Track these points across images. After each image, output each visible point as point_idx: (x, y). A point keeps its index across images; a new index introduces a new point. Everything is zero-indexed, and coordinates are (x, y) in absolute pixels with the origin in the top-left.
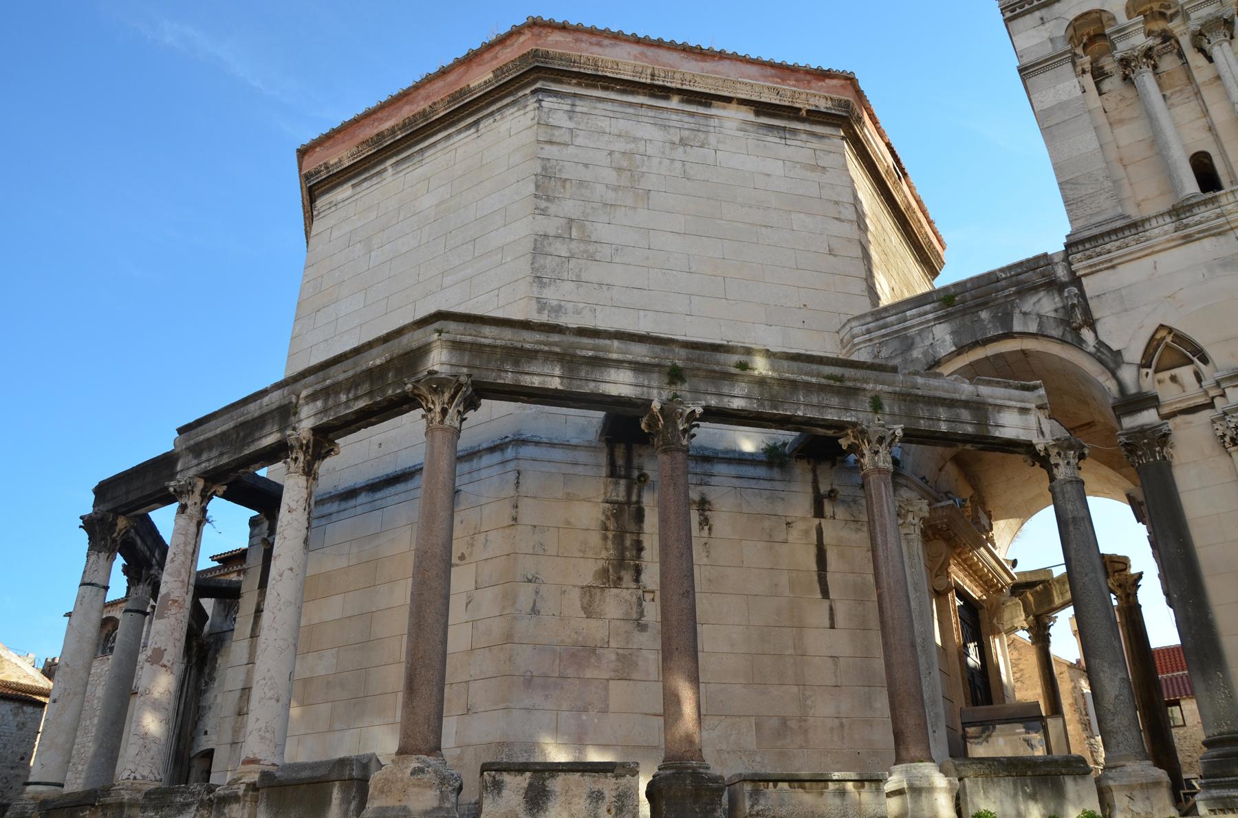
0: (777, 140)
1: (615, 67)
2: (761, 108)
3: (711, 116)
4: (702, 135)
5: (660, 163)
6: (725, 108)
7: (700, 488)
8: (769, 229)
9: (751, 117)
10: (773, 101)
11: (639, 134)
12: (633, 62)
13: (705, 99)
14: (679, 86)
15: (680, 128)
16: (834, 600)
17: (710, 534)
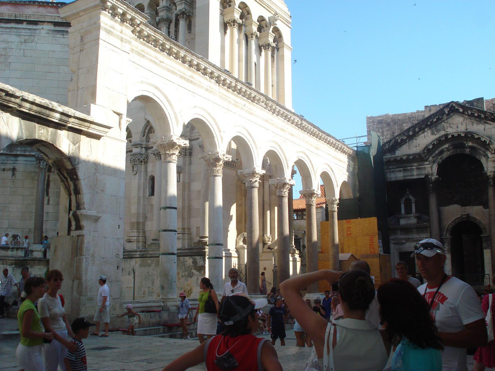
0: (60, 36)
1: (2, 15)
2: (56, 24)
3: (37, 29)
4: (32, 37)
5: (16, 51)
6: (43, 25)
7: (13, 165)
8: (51, 74)
9: (52, 27)
10: (60, 21)
11: (10, 40)
12: (7, 12)
13: (35, 23)
14: (25, 19)
15: (25, 35)
16: (50, 197)
17: (15, 178)
